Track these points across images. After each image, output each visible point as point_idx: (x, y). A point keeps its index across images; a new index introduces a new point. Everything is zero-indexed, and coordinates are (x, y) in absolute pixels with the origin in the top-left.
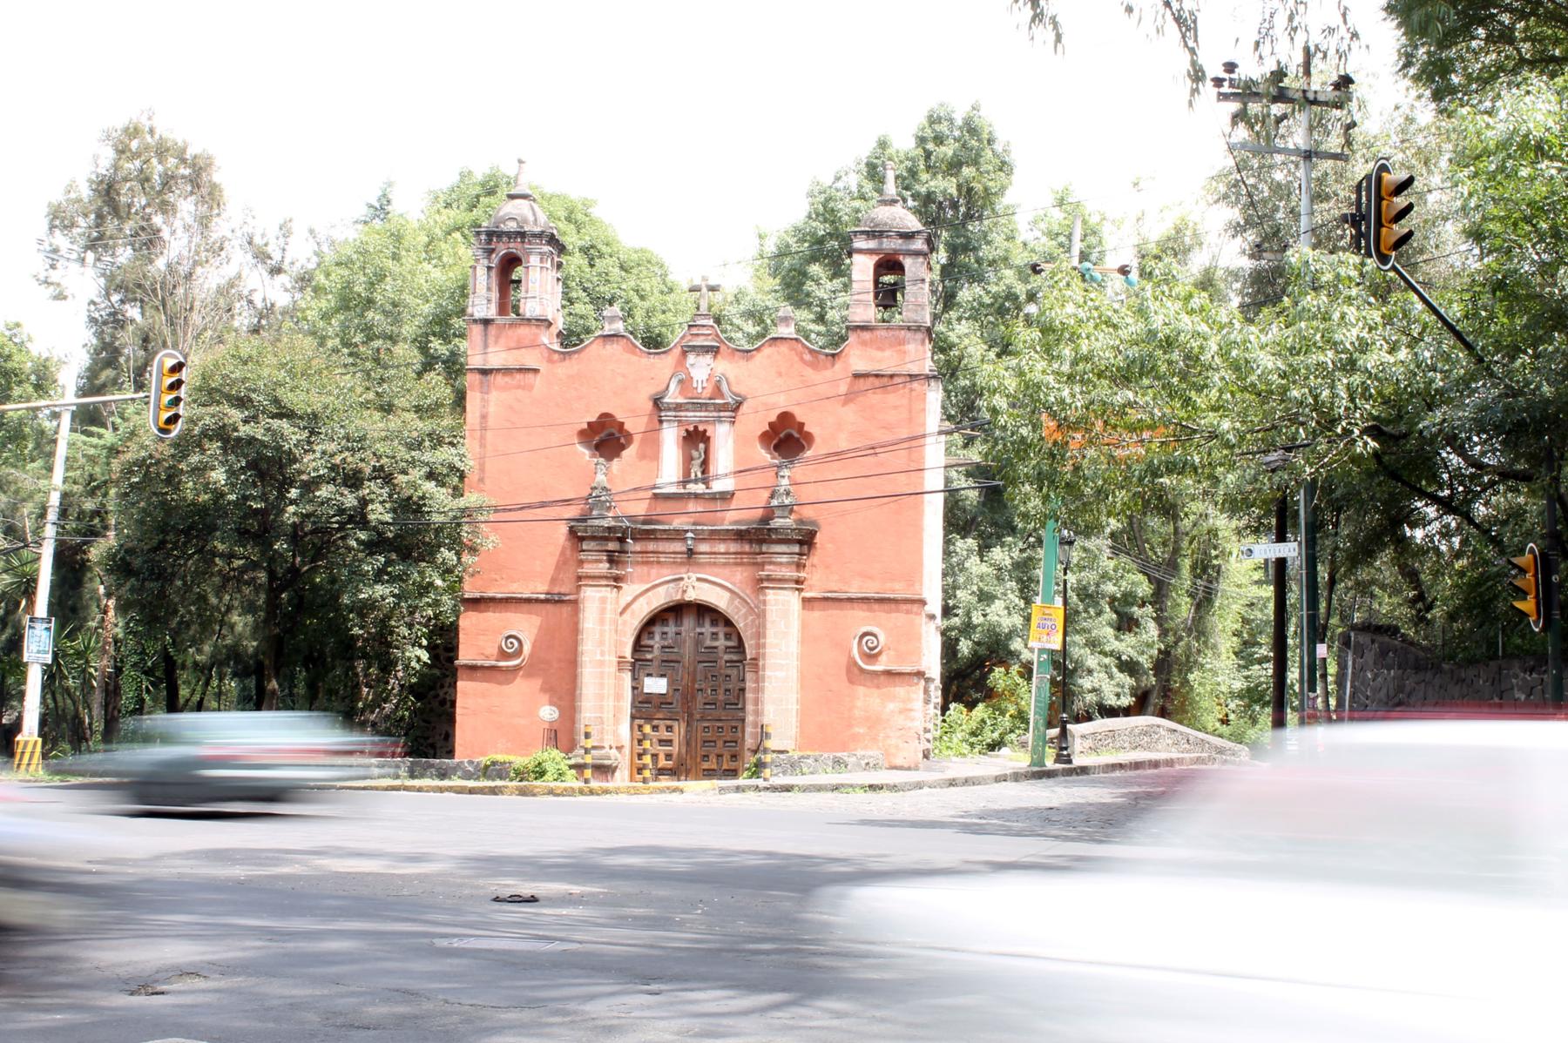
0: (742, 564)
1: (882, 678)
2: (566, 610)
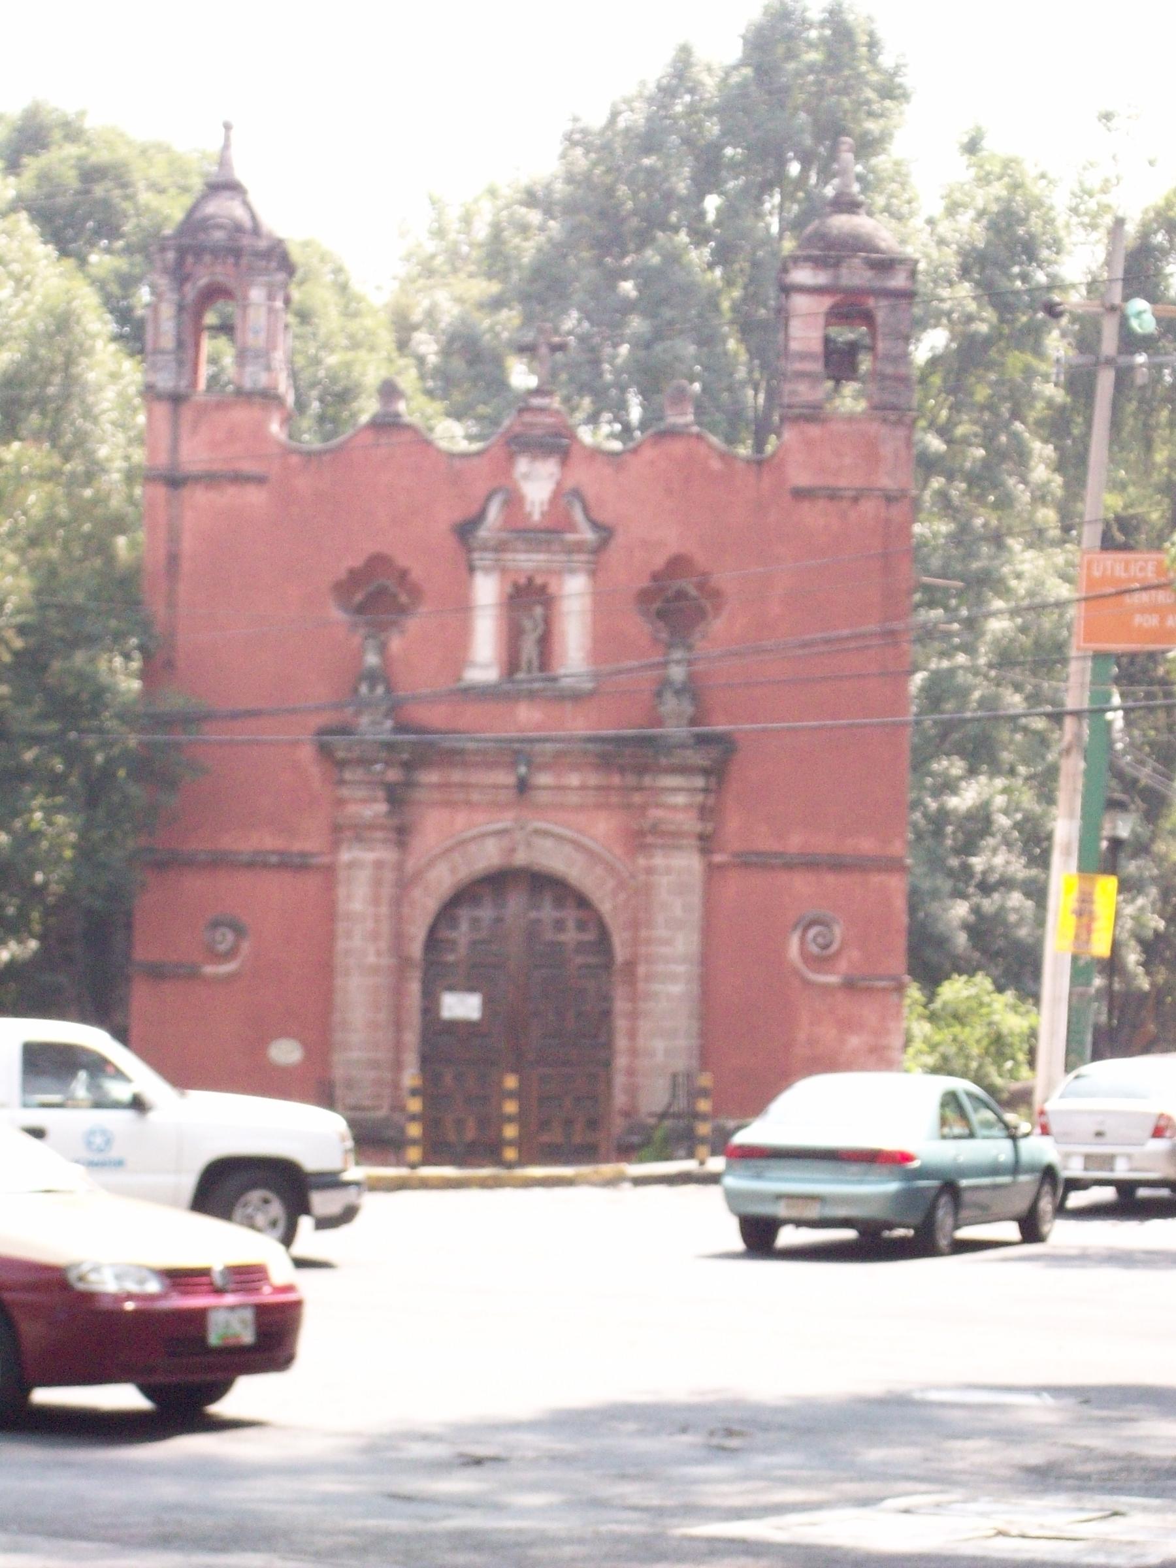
2: (311, 883)
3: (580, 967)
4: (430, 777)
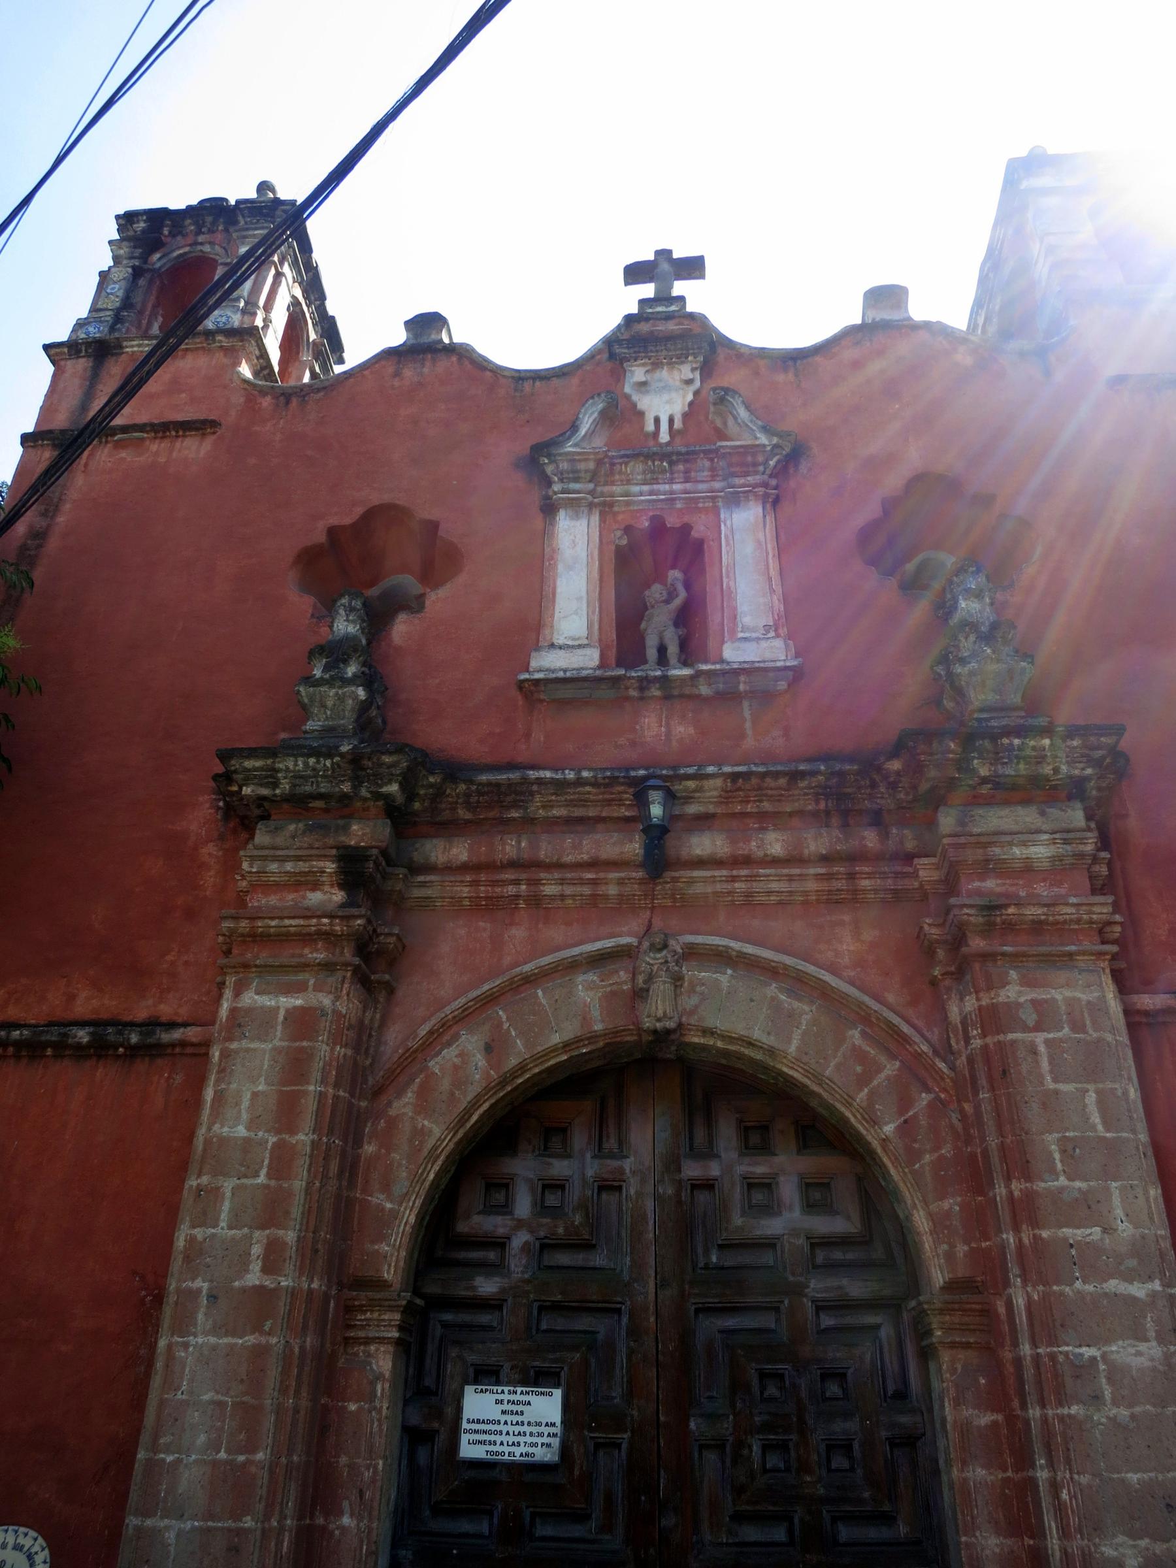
0: (854, 898)
3: (821, 1307)
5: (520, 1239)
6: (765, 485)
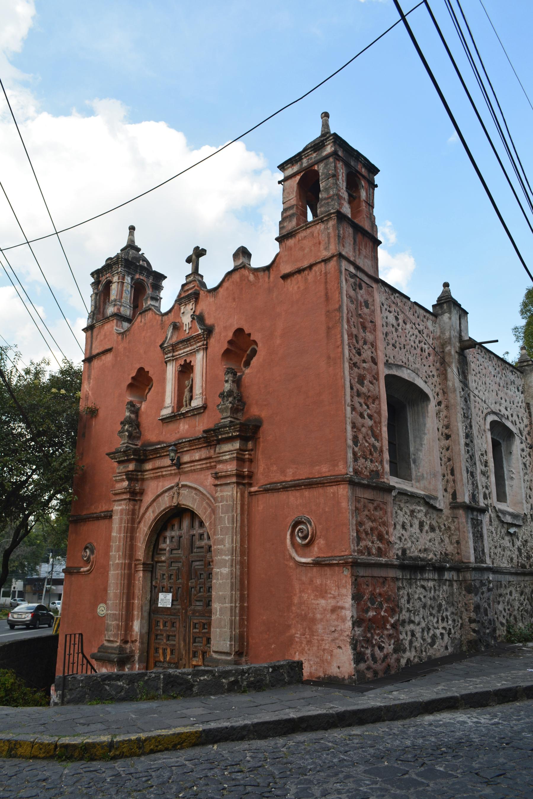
0: (211, 468)
1: (315, 569)
4: (149, 466)
5: (168, 549)
6: (203, 345)
